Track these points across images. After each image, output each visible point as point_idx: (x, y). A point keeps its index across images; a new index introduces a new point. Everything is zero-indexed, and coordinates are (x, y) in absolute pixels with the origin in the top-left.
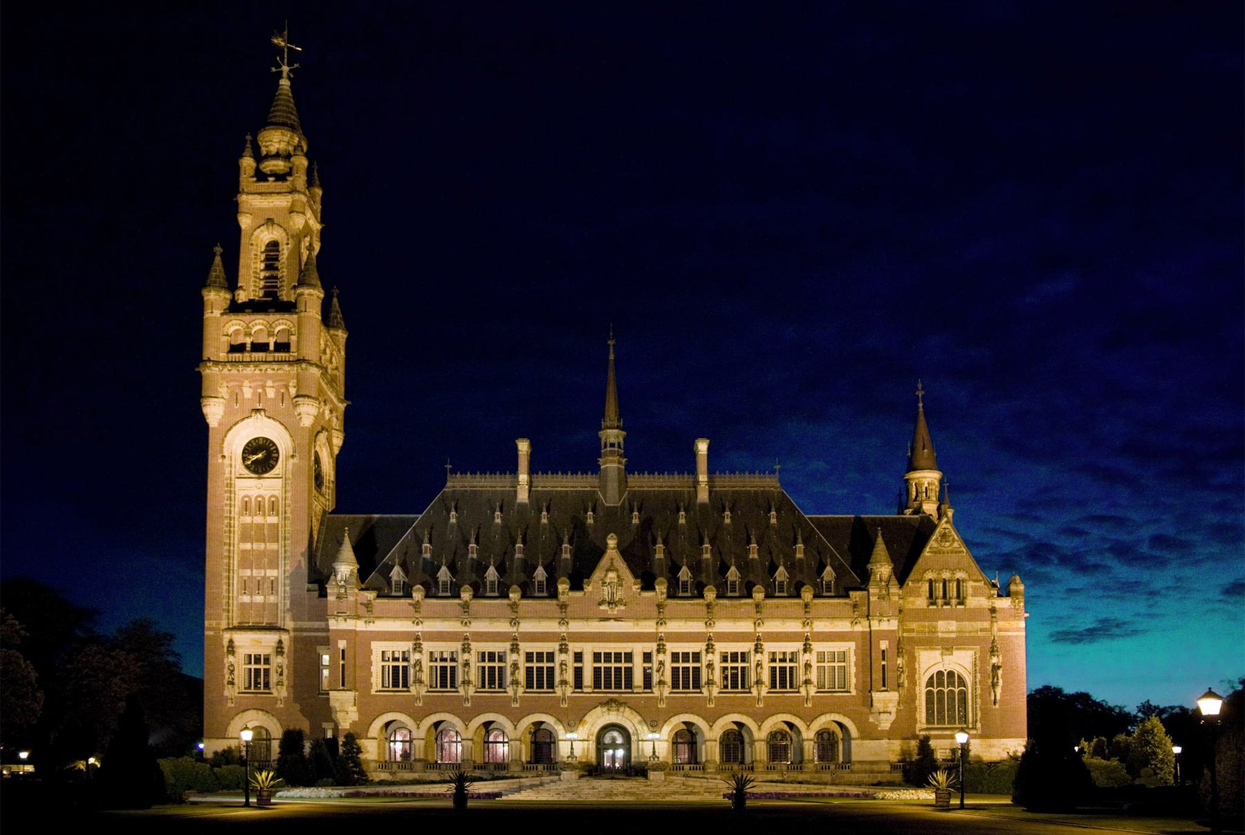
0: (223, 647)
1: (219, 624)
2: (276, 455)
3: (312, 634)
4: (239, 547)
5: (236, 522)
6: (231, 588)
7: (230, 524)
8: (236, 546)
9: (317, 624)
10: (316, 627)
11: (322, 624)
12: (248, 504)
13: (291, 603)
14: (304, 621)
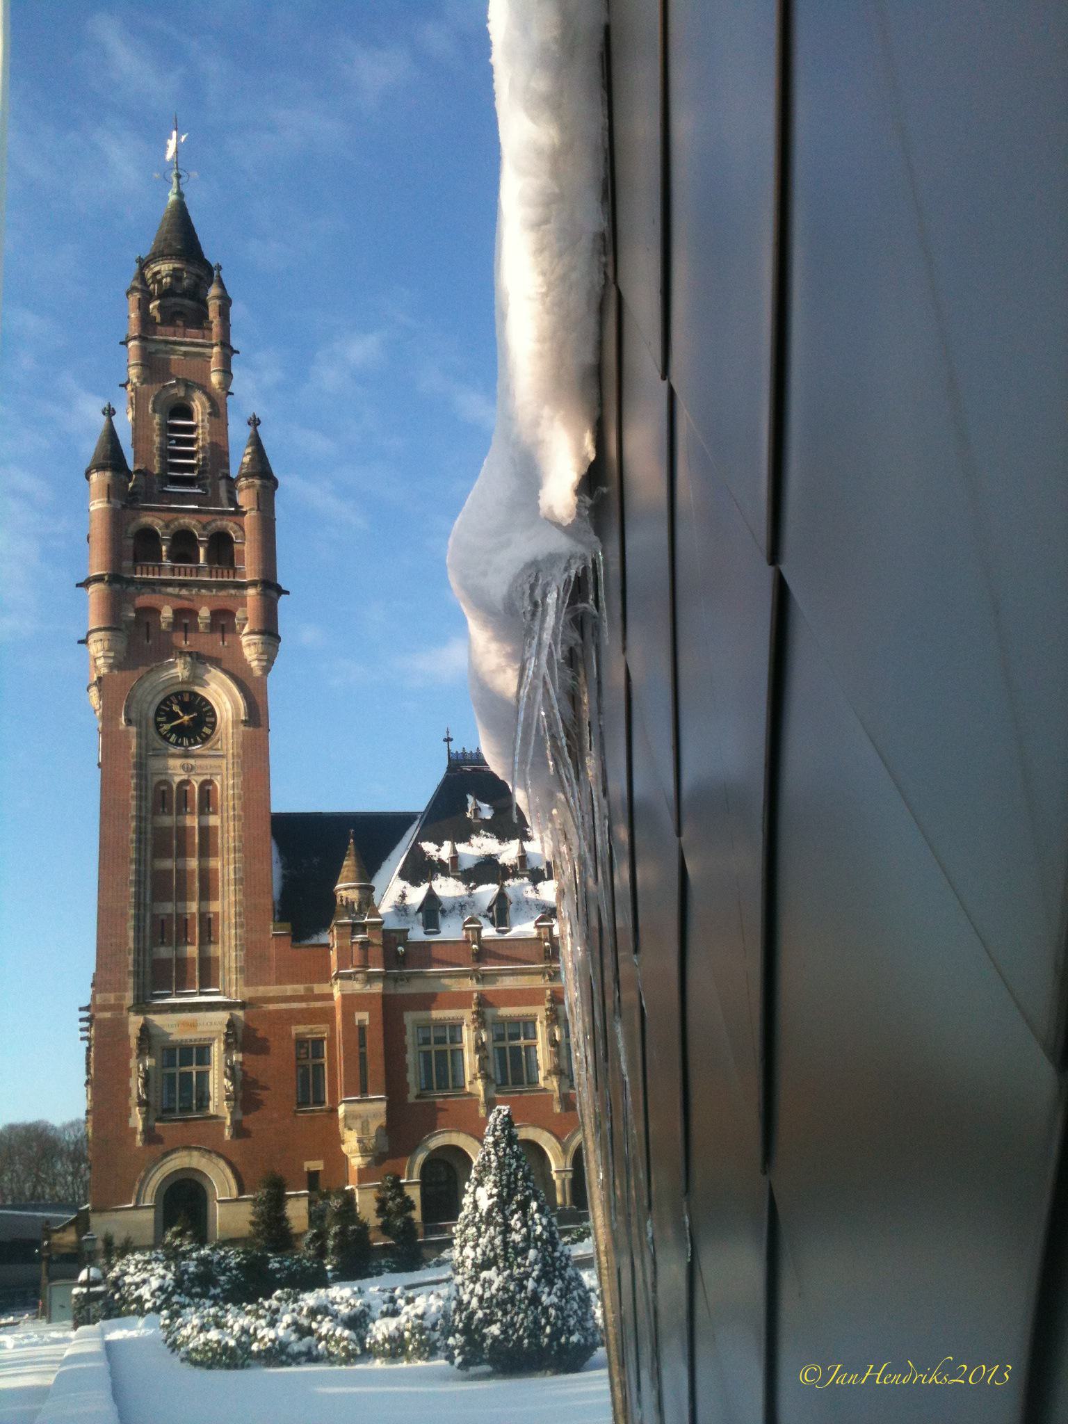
0: (128, 1037)
1: (122, 998)
2: (213, 720)
3: (284, 1006)
4: (152, 866)
5: (149, 827)
6: (142, 934)
7: (140, 828)
8: (149, 863)
9: (289, 989)
10: (289, 993)
11: (300, 989)
12: (167, 796)
13: (246, 955)
14: (267, 984)
